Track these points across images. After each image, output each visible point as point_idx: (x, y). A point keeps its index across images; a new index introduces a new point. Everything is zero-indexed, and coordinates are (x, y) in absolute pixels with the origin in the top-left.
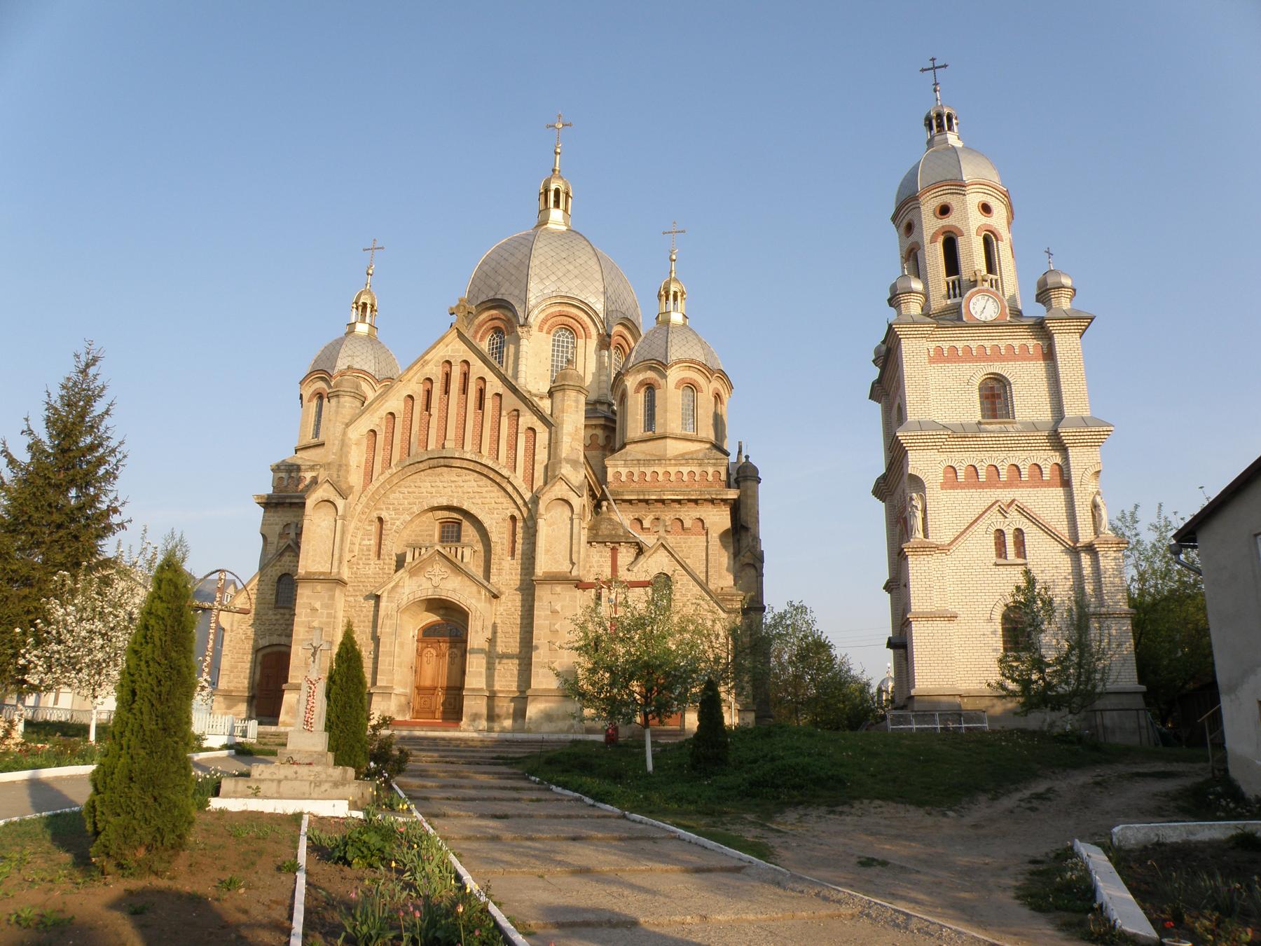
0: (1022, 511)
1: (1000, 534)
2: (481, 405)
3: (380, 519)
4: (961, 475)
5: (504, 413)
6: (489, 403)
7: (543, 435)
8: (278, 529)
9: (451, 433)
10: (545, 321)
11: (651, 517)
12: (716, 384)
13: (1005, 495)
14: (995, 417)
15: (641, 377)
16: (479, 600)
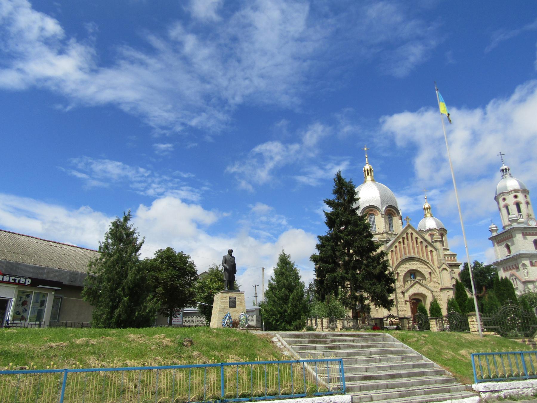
3: (398, 273)
6: (419, 244)
7: (434, 253)
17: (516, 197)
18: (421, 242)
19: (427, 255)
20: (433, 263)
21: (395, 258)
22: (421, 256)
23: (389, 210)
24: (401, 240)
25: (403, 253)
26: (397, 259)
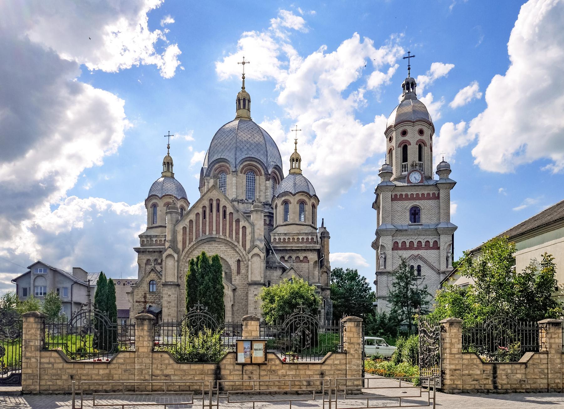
2: (225, 216)
4: (400, 245)
5: (234, 220)
7: (249, 230)
9: (214, 229)
10: (243, 168)
11: (288, 256)
12: (313, 201)
14: (415, 222)
15: (283, 198)
16: (229, 291)
18: (231, 214)
19: (237, 233)
20: (244, 246)
21: (188, 238)
22: (227, 235)
23: (249, 165)
24: (200, 211)
25: (201, 230)
26: (191, 240)
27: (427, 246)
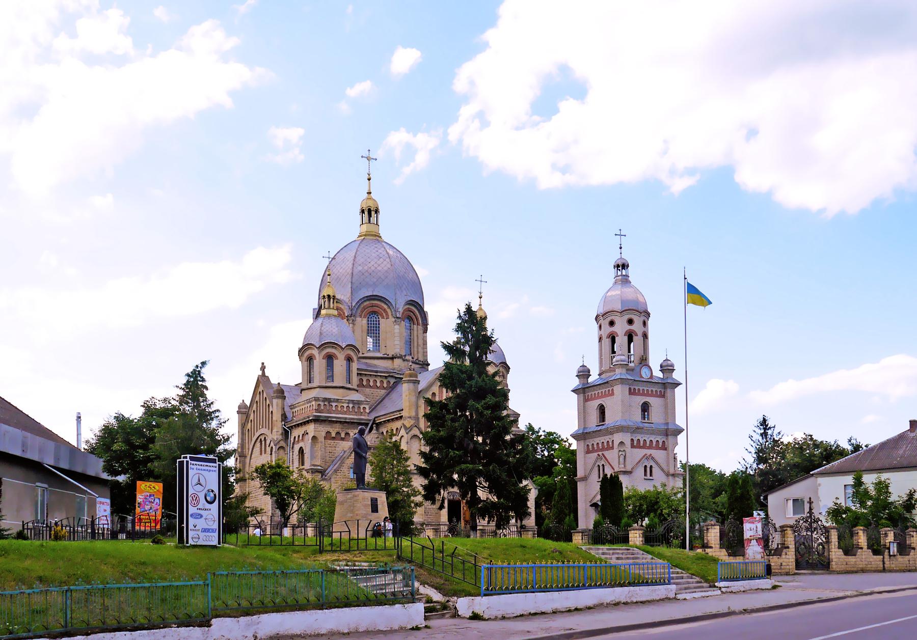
0: (653, 458)
1: (646, 467)
8: (324, 434)
13: (648, 452)
17: (630, 322)
27: (657, 448)
